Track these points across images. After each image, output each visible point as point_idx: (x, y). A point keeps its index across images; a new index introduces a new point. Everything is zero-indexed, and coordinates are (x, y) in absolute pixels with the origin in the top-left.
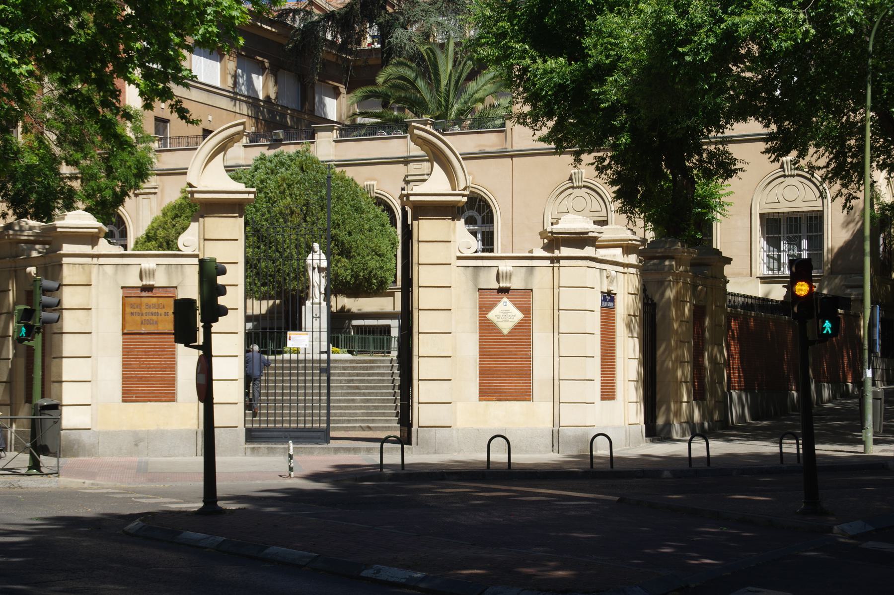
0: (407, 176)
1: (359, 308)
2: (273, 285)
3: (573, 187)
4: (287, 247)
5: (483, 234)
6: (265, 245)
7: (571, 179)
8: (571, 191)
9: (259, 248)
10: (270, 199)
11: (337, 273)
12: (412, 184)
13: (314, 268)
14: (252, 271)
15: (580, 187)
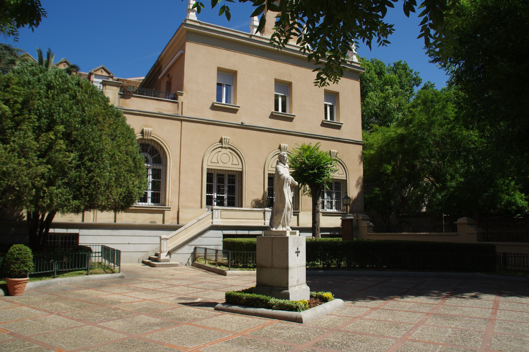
3: (222, 147)
5: (153, 170)
7: (221, 141)
8: (220, 149)
15: (226, 148)
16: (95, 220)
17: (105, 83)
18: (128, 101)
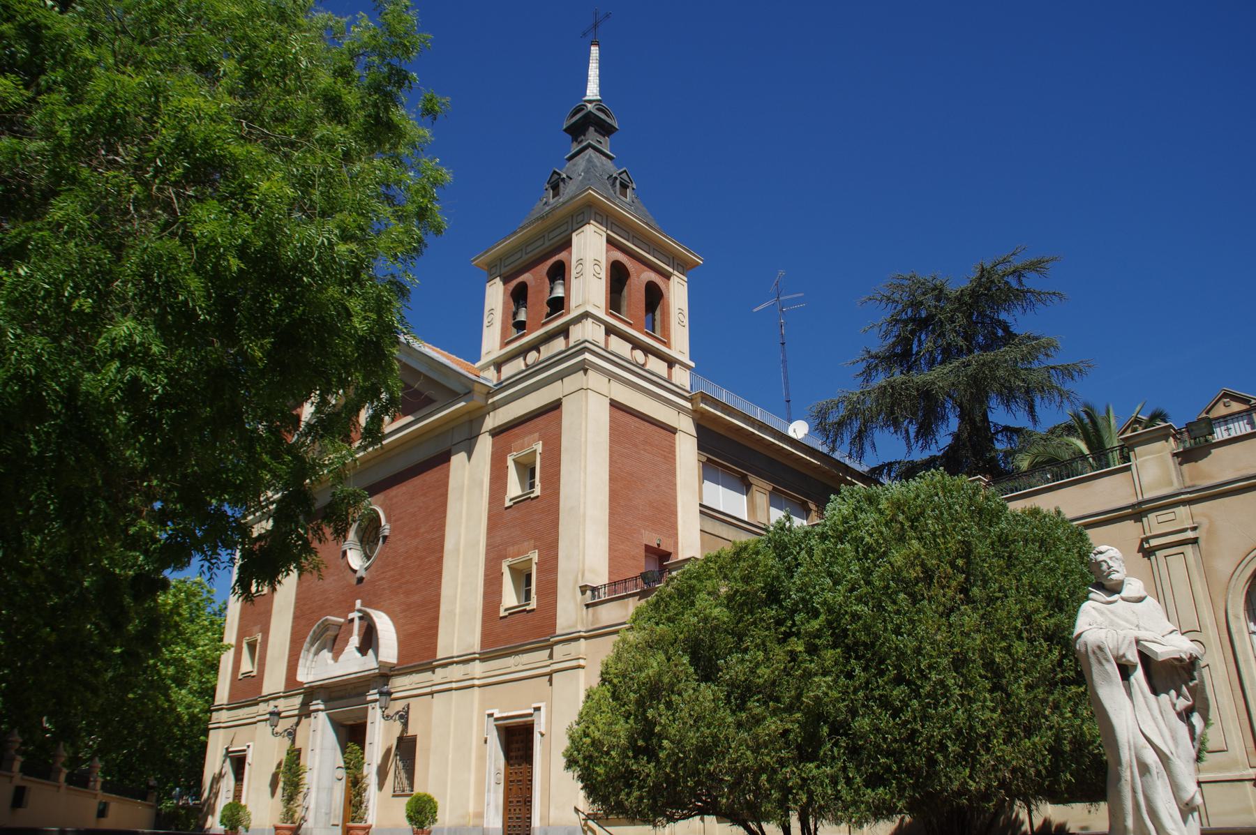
0: (1147, 540)
1: (1084, 824)
2: (899, 781)
4: (930, 667)
6: (865, 669)
9: (850, 675)
10: (870, 549)
11: (1082, 734)
12: (1160, 554)
13: (1125, 671)
14: (836, 744)
16: (1204, 820)
17: (1131, 442)
18: (1203, 464)
